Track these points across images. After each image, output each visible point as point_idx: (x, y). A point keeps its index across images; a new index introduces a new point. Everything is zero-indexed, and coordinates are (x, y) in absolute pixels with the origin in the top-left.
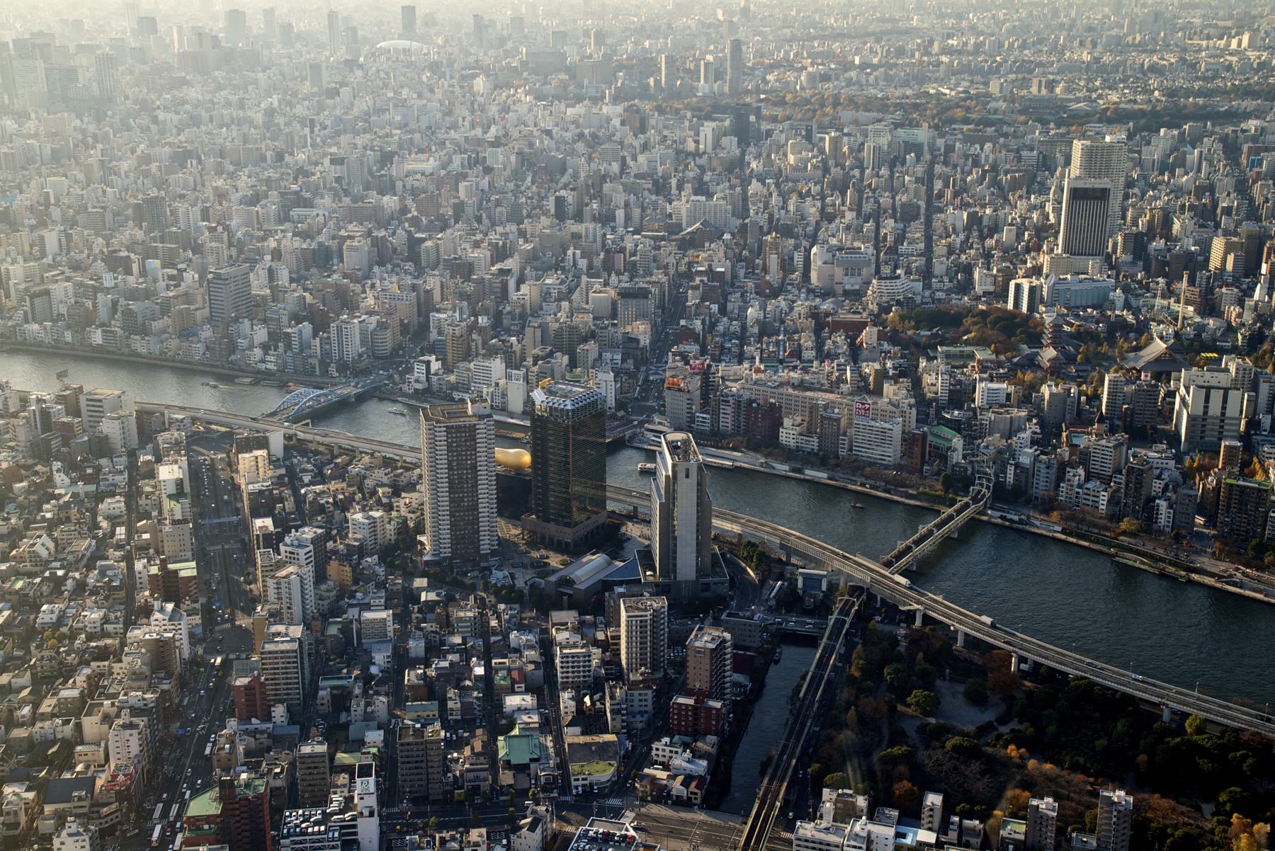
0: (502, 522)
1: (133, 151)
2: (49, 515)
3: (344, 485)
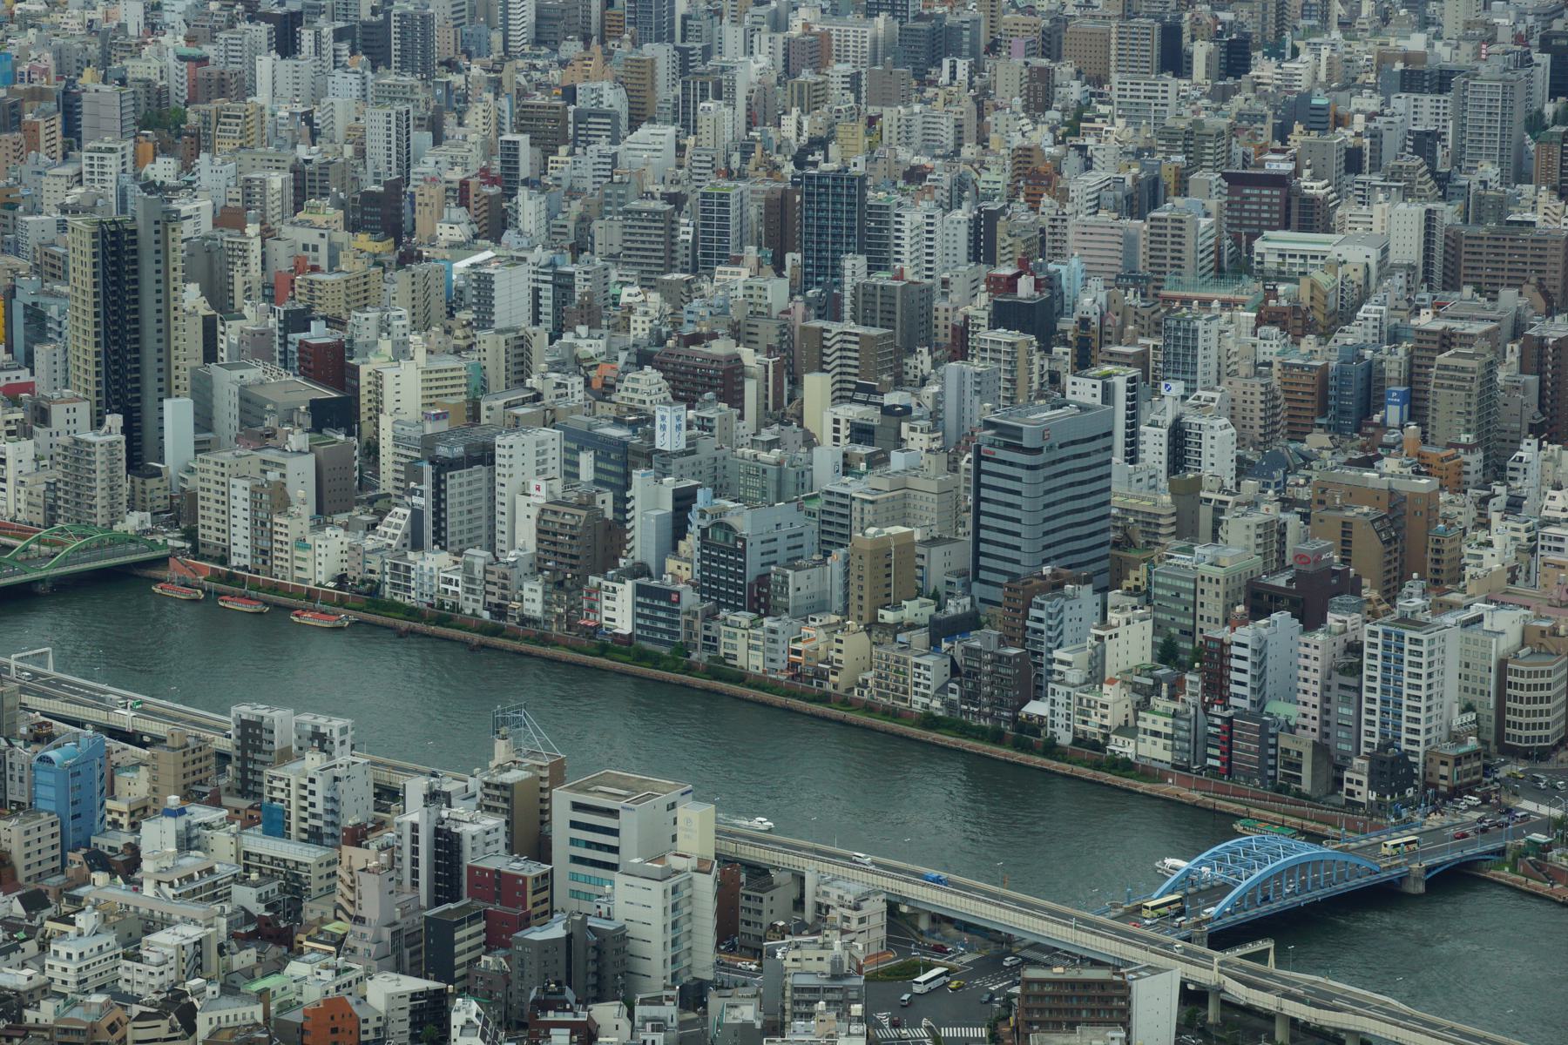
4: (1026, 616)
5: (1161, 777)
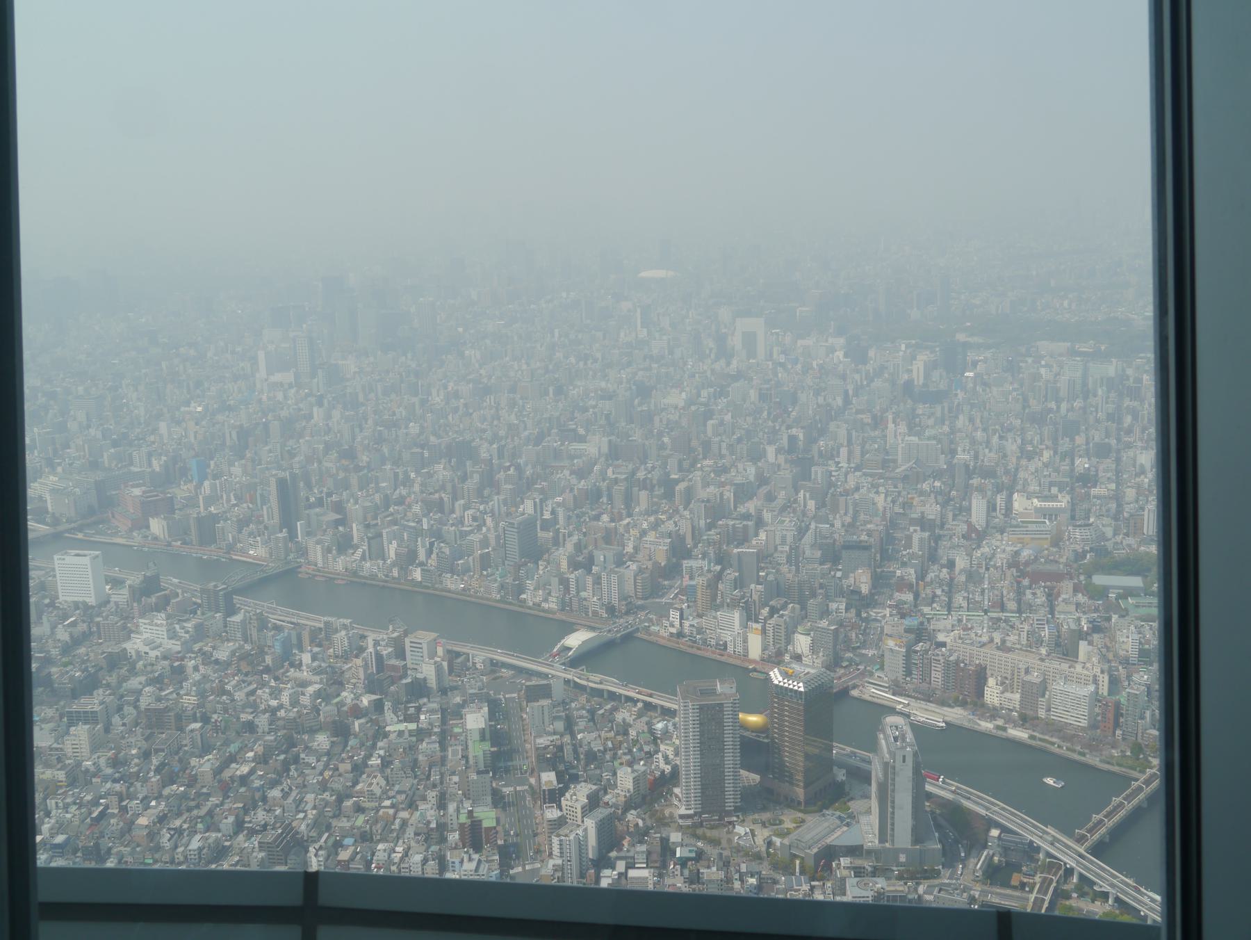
2: (382, 752)
3: (612, 734)
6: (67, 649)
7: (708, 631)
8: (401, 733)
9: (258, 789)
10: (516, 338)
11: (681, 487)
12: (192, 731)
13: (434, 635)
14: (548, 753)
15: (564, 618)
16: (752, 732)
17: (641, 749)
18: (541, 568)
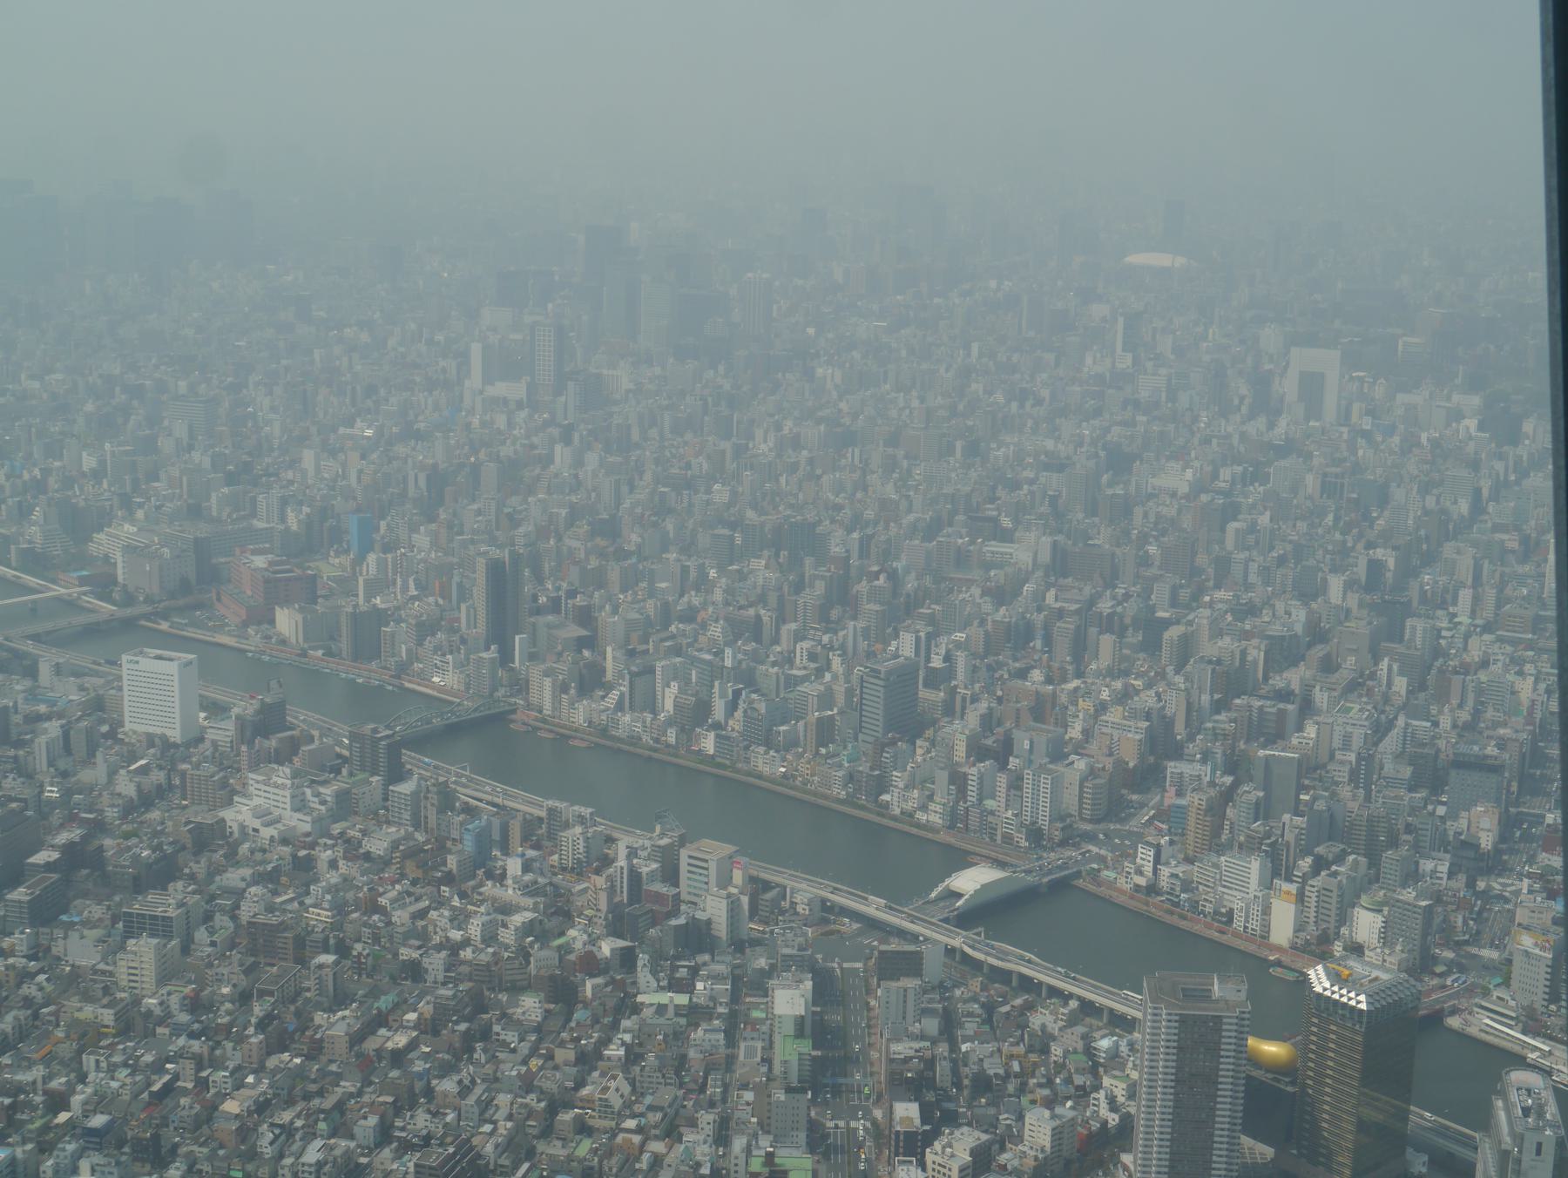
0: (1246, 1141)
1: (779, 428)
2: (627, 1038)
3: (1021, 1049)
4: (882, 756)
5: (938, 832)
6: (130, 809)
7: (1201, 887)
8: (661, 1009)
9: (420, 1076)
10: (904, 353)
11: (1173, 633)
12: (321, 966)
13: (728, 849)
14: (909, 1071)
15: (952, 841)
16: (1268, 1071)
17: (1068, 1081)
18: (919, 751)
